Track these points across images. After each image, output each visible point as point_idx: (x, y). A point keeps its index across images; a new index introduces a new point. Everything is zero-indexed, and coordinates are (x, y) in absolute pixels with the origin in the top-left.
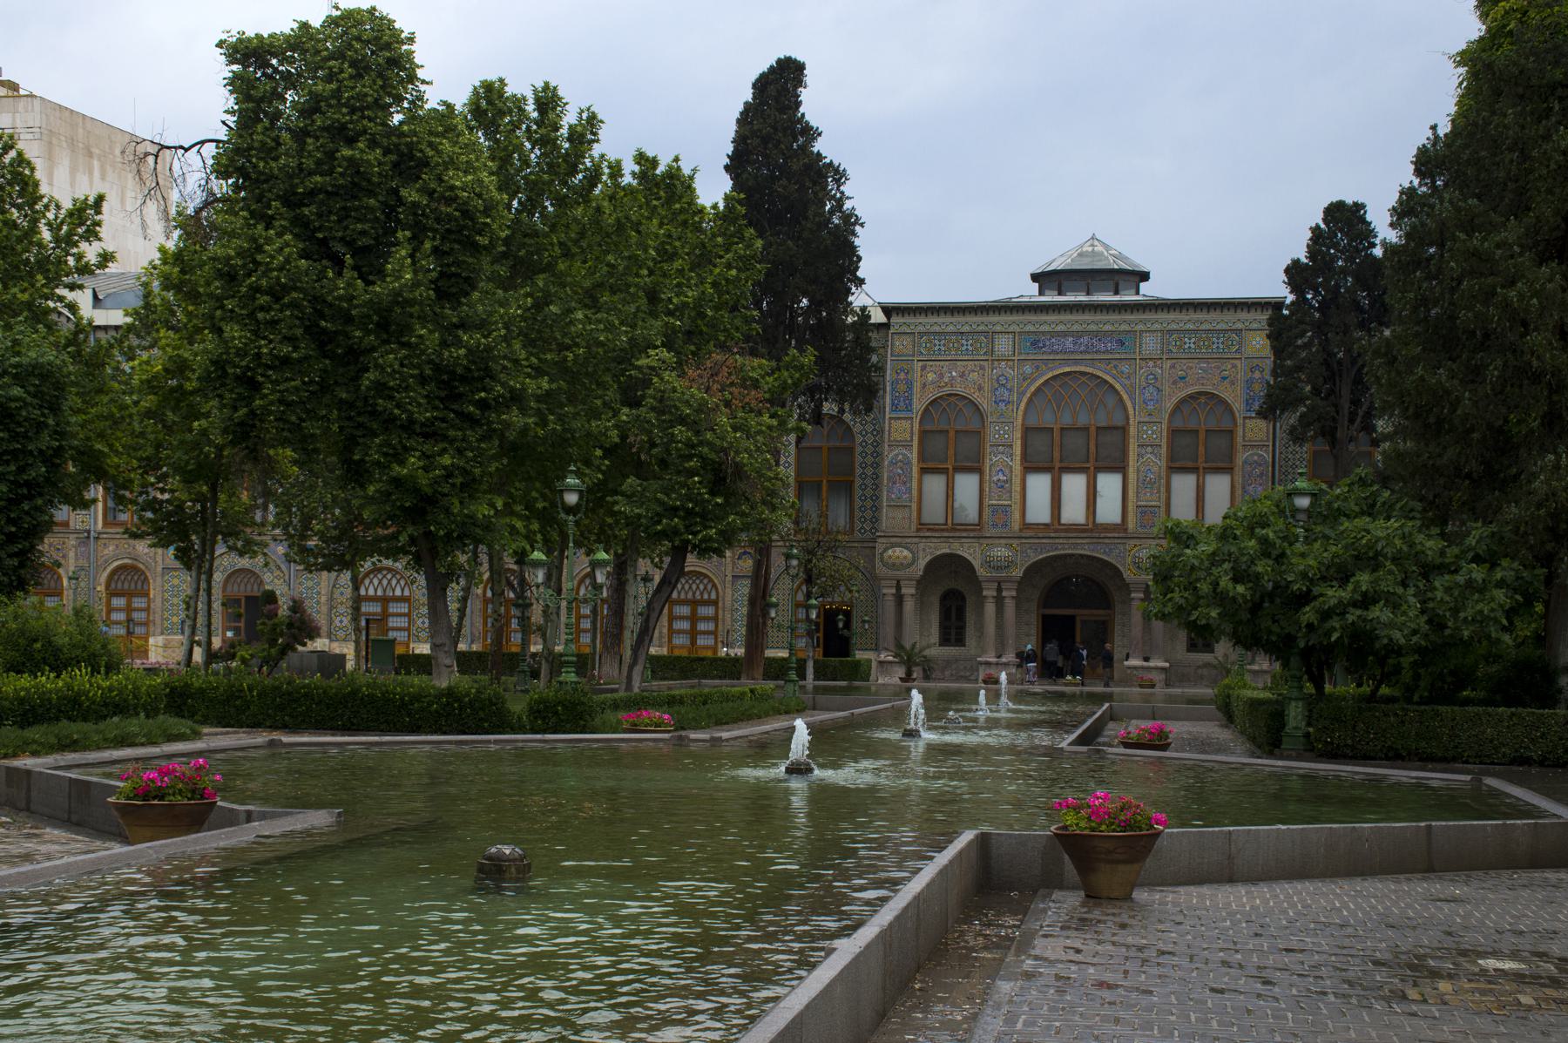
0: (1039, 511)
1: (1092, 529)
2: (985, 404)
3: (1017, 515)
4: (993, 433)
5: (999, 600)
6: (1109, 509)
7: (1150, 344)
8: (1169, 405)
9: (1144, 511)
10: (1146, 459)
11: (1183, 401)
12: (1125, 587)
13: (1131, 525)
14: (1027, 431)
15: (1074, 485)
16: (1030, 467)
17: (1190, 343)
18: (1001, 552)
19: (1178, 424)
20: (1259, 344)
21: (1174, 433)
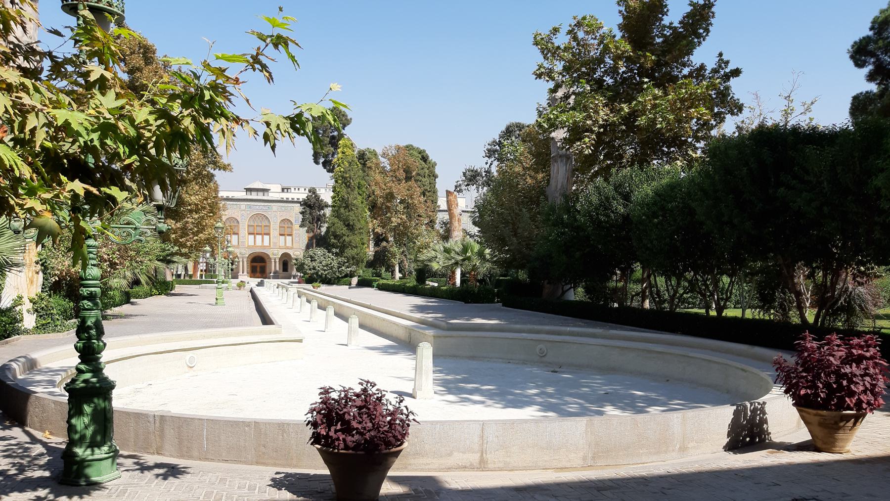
0: (251, 243)
1: (265, 247)
2: (239, 220)
3: (246, 244)
4: (241, 225)
5: (243, 261)
6: (266, 243)
7: (275, 208)
8: (279, 221)
9: (275, 243)
10: (274, 231)
11: (282, 220)
12: (270, 259)
13: (272, 246)
14: (249, 226)
15: (259, 237)
16: (249, 234)
17: (283, 209)
18: (243, 251)
19: (281, 225)
20: (298, 208)
21: (280, 227)
